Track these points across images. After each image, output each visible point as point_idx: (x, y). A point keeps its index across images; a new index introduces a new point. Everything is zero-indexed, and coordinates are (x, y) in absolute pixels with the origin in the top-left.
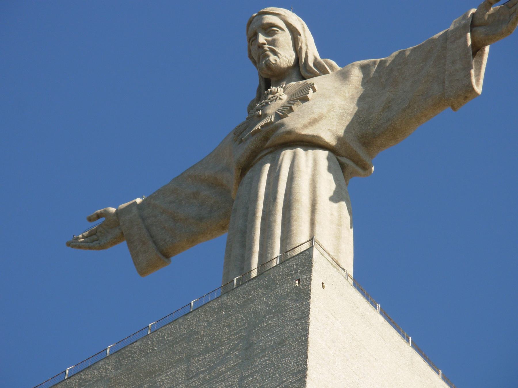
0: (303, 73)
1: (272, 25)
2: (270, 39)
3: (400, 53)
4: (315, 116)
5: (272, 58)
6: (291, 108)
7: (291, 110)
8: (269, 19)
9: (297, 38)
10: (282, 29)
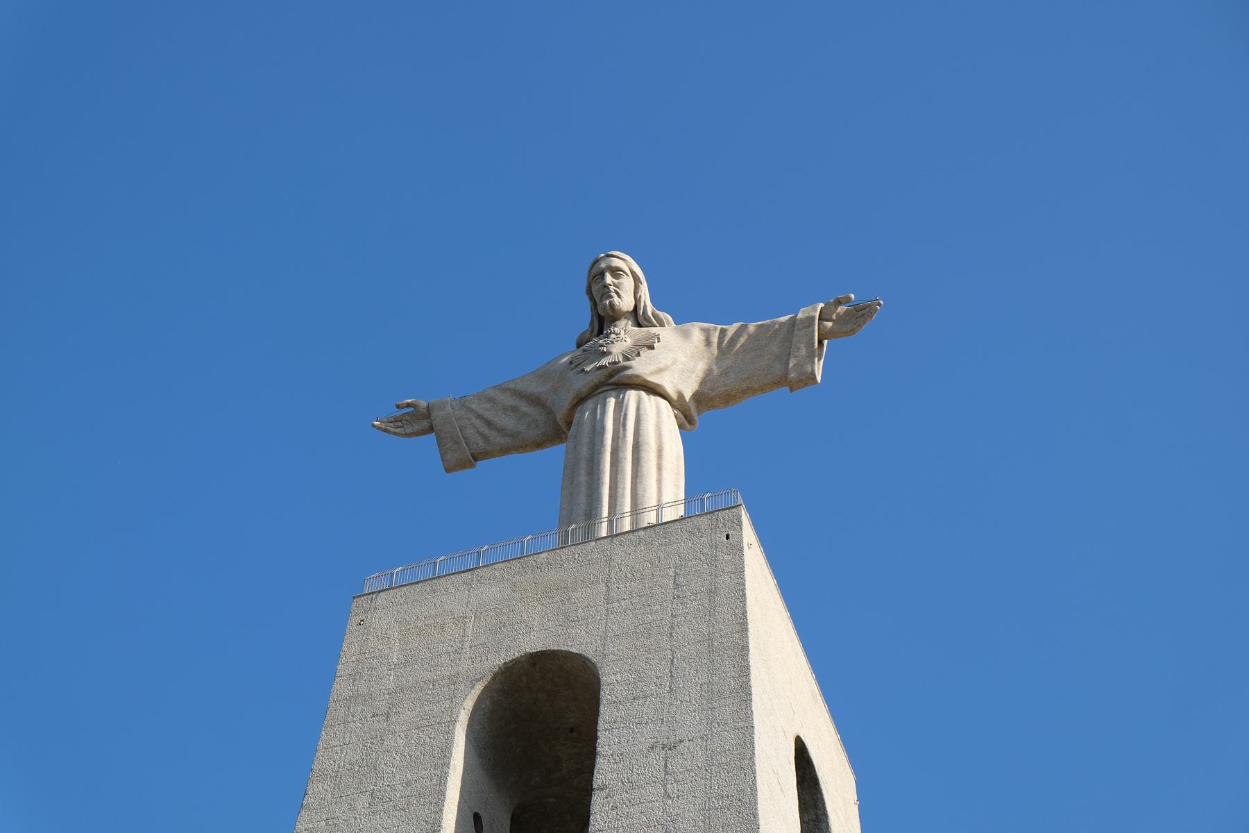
0: (641, 320)
1: (619, 269)
2: (616, 281)
3: (742, 325)
4: (662, 366)
5: (616, 300)
6: (639, 353)
7: (639, 354)
8: (616, 263)
9: (639, 286)
10: (627, 275)
